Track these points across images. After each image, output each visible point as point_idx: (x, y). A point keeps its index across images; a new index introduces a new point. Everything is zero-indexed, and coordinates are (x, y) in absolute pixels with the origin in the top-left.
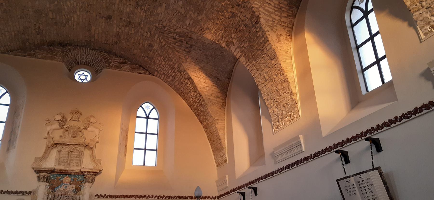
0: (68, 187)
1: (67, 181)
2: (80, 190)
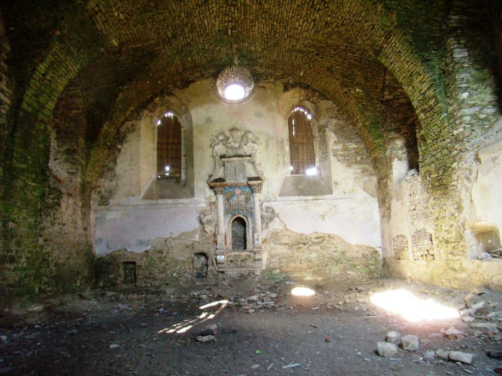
2: (250, 200)
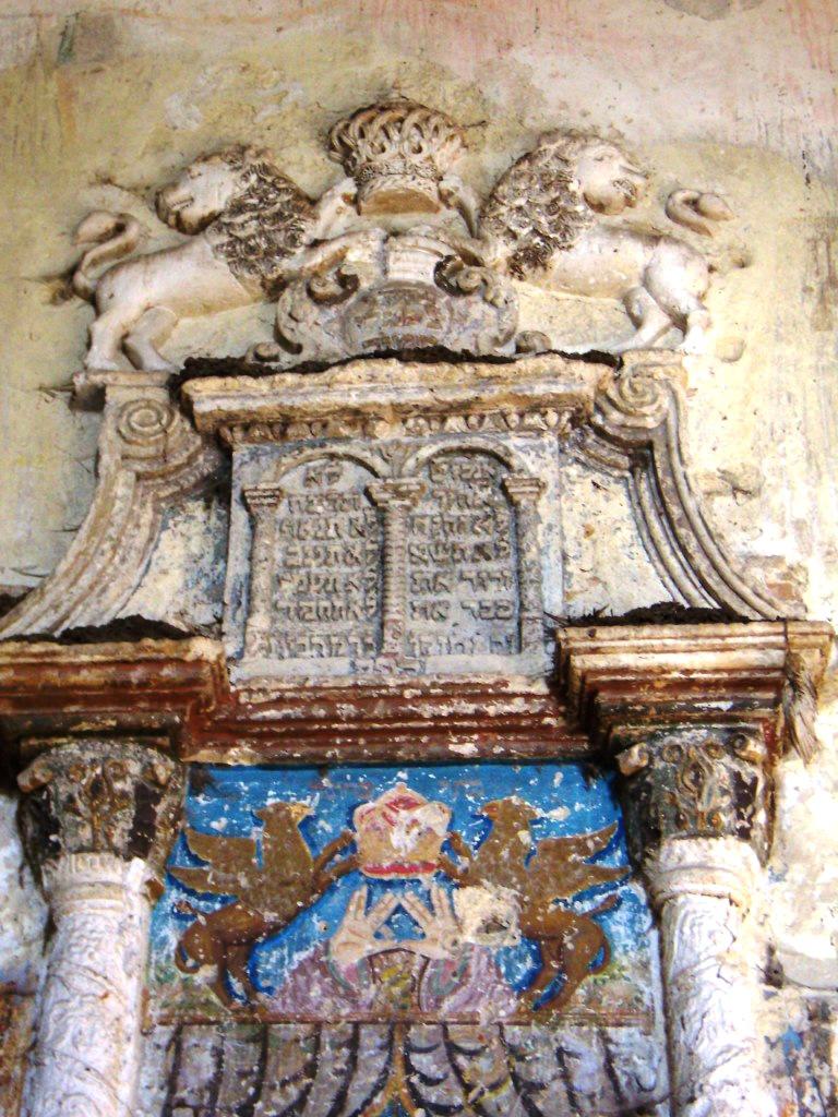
0: (436, 926)
1: (402, 841)
